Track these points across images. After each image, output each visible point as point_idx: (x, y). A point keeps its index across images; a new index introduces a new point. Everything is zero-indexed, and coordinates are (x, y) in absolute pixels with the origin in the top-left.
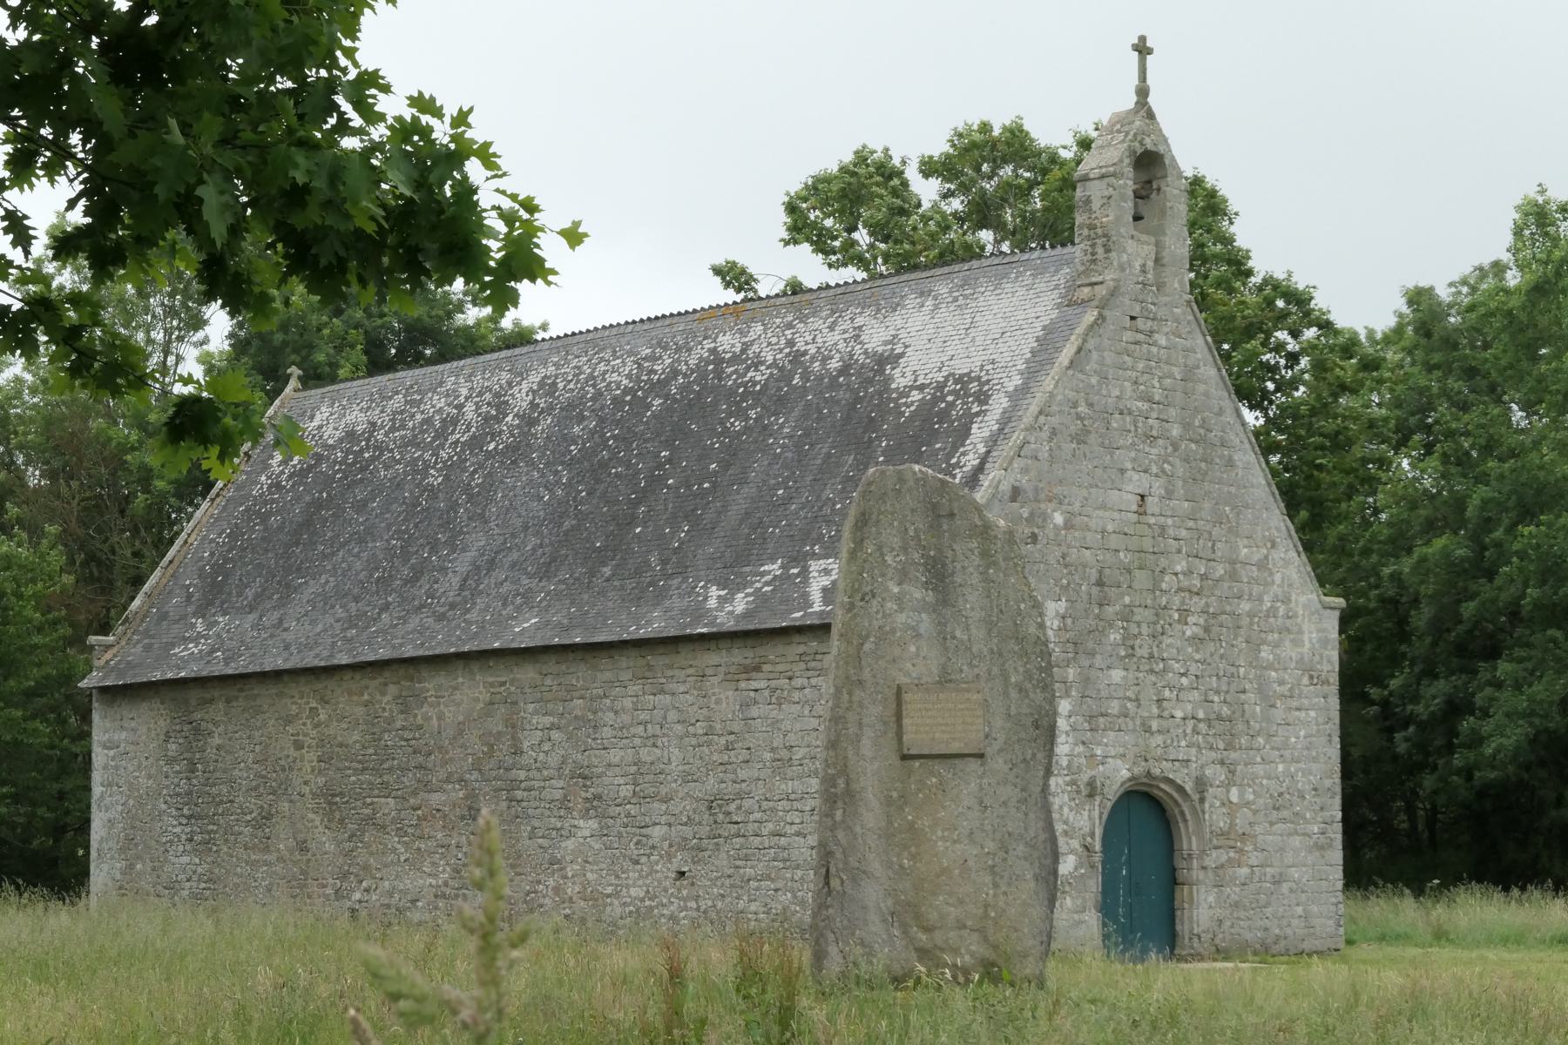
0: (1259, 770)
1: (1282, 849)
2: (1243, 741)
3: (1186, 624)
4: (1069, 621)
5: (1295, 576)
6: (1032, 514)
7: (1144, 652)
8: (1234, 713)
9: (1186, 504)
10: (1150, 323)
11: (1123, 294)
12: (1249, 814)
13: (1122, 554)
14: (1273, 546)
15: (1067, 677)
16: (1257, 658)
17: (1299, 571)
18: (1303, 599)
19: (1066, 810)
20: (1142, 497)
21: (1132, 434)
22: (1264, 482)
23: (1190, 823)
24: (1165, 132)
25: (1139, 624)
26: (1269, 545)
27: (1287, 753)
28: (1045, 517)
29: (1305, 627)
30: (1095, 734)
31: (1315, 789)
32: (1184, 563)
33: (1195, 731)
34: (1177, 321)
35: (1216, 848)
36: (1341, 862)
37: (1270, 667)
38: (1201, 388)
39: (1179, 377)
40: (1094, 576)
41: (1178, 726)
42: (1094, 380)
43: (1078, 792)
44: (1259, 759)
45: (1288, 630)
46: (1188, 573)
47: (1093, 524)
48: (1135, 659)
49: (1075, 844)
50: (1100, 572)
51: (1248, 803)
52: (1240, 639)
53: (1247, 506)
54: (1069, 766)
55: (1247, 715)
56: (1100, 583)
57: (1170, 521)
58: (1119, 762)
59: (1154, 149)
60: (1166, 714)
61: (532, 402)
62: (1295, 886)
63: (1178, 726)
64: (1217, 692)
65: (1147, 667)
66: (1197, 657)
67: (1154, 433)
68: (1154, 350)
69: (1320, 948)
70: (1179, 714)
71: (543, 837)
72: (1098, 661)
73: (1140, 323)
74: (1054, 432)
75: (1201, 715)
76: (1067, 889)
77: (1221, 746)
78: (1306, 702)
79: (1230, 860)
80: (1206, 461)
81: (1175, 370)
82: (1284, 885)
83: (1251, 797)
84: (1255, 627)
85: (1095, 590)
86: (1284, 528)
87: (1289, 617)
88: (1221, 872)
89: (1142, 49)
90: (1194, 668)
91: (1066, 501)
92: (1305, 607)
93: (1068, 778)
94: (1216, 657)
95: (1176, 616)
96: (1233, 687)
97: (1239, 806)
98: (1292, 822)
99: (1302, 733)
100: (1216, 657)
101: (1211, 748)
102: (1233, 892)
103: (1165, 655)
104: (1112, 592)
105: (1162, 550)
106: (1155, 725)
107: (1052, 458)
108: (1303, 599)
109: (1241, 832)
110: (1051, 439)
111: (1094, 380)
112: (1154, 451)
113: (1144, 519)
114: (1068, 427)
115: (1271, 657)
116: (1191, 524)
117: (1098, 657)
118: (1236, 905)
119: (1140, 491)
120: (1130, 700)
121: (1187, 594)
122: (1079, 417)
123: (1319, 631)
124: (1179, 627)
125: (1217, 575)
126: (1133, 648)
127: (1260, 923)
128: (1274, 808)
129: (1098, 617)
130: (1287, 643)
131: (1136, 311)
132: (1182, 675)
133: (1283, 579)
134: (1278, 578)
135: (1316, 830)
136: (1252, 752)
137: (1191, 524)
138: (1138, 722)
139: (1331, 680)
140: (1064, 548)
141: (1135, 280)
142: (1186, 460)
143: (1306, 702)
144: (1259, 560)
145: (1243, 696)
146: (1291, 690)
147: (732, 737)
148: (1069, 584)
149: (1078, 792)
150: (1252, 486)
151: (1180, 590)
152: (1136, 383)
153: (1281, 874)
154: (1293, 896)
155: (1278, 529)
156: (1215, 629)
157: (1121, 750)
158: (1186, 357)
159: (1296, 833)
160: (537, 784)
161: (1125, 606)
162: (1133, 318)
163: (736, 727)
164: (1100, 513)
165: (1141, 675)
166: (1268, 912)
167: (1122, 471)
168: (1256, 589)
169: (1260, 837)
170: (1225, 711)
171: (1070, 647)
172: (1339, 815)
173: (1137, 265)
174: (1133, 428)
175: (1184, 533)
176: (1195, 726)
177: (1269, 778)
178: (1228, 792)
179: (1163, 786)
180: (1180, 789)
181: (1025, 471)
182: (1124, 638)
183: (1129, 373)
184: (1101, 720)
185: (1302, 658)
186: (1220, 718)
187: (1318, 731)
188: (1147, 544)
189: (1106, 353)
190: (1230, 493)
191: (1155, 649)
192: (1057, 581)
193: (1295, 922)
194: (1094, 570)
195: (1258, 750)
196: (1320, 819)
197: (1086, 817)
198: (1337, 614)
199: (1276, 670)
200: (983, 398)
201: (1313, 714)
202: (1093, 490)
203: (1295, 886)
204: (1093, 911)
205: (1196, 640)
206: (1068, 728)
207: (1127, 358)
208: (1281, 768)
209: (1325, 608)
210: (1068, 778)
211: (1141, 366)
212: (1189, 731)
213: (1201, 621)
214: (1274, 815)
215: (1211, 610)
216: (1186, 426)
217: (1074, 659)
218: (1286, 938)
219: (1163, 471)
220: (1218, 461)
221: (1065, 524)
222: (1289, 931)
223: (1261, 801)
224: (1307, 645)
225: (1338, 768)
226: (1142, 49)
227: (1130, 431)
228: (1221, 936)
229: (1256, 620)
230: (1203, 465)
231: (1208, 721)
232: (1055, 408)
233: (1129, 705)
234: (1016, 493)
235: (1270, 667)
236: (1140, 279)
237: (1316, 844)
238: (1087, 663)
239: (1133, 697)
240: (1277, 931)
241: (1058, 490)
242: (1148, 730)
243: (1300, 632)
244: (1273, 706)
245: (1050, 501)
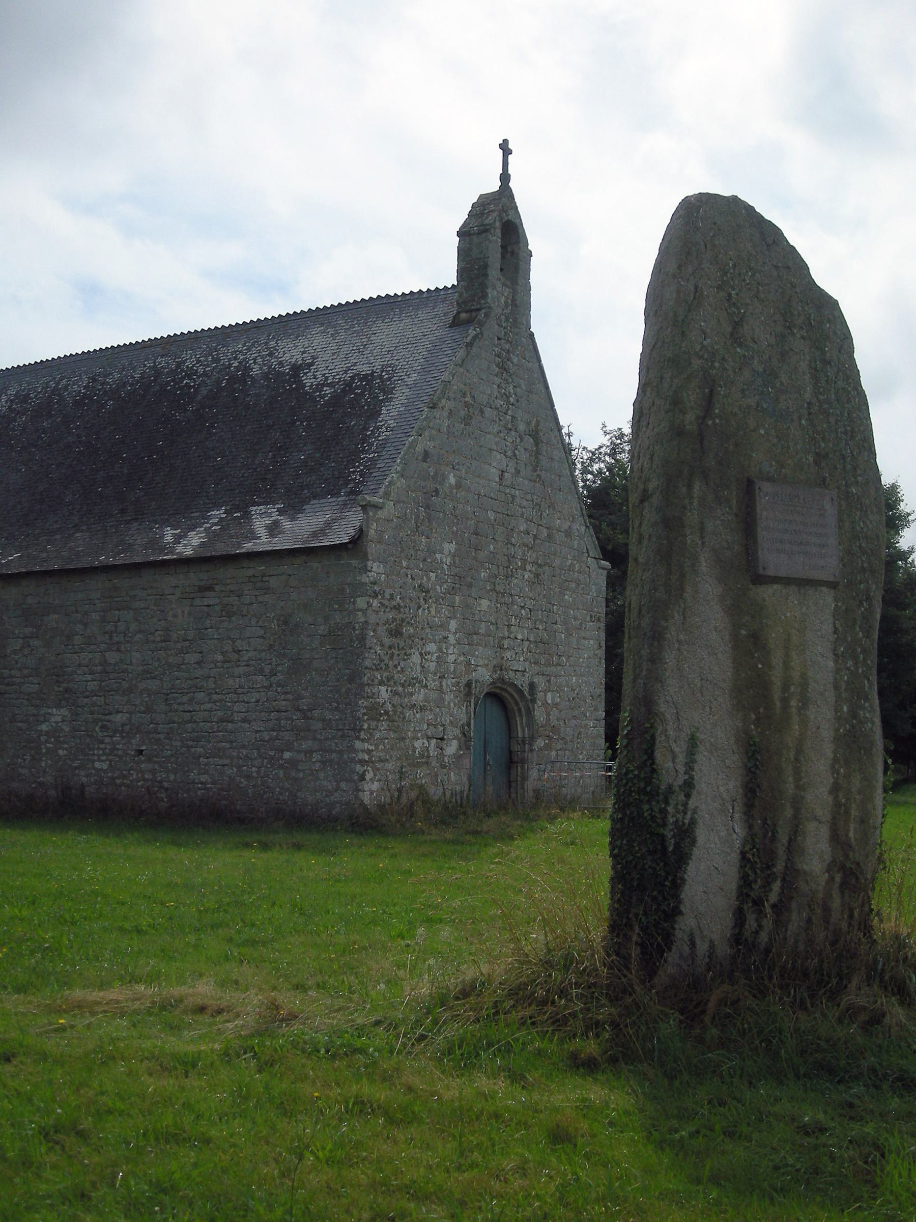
6: (436, 473)
15: (454, 603)
19: (452, 705)
23: (524, 718)
28: (444, 478)
31: (591, 696)
49: (457, 732)
60: (512, 636)
61: (10, 407)
70: (520, 637)
71: (22, 722)
75: (532, 639)
89: (505, 148)
90: (529, 604)
93: (453, 681)
94: (541, 596)
100: (541, 596)
106: (506, 643)
119: (501, 468)
136: (559, 668)
146: (581, 624)
147: (187, 644)
149: (460, 692)
160: (18, 680)
163: (191, 634)
175: (525, 503)
178: (546, 696)
181: (431, 438)
182: (489, 576)
184: (475, 637)
200: (388, 391)
201: (592, 642)
221: (456, 485)
226: (505, 148)
234: (426, 455)
242: (501, 647)
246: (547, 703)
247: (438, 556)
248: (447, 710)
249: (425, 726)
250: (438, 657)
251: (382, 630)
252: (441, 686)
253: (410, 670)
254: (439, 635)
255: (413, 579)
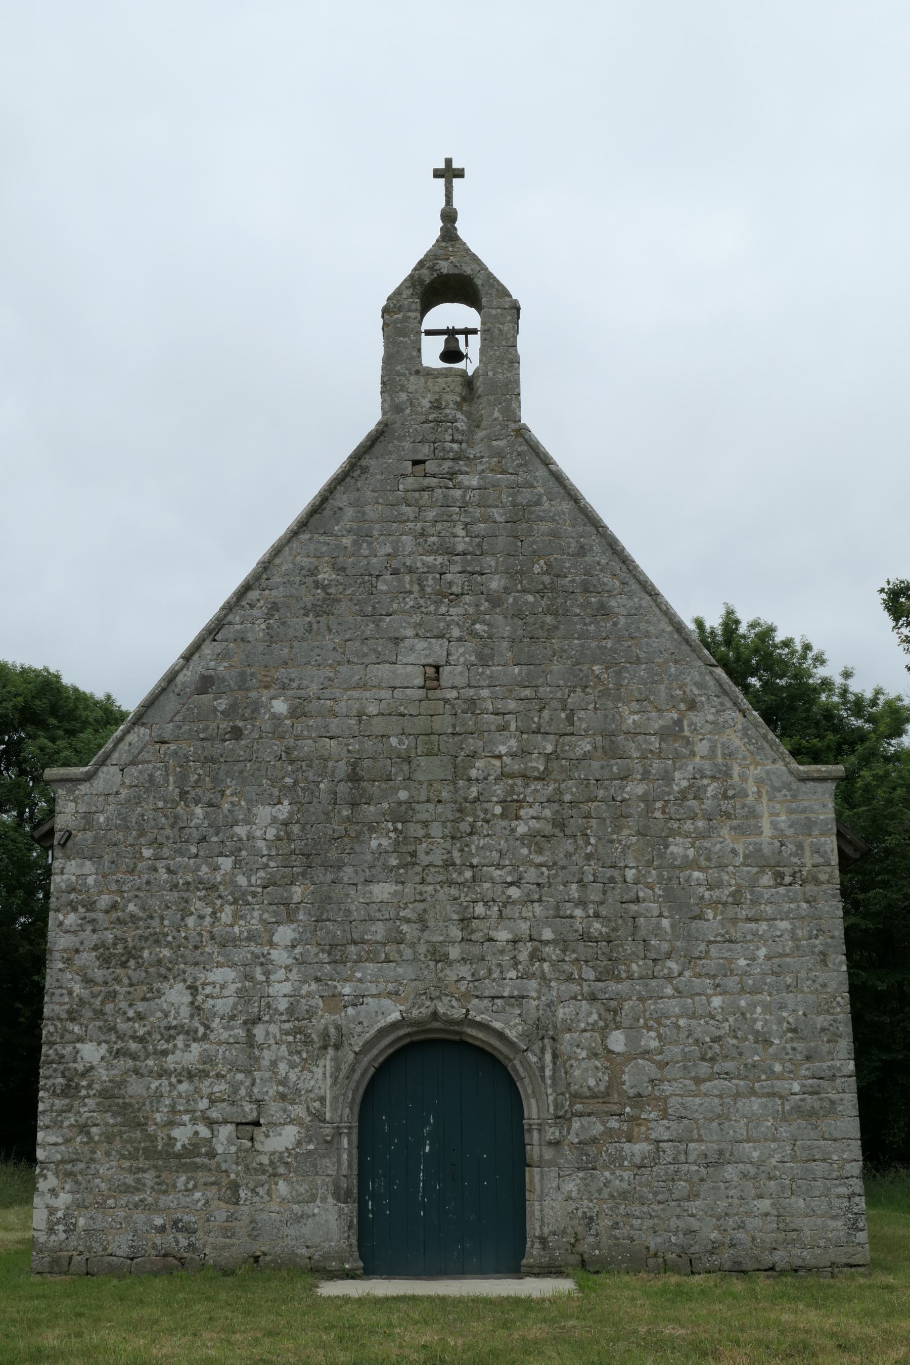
0: (674, 1006)
1: (722, 1118)
2: (634, 967)
3: (518, 818)
4: (296, 829)
5: (737, 742)
6: (233, 707)
7: (437, 858)
8: (615, 930)
9: (517, 669)
10: (449, 463)
11: (401, 439)
12: (651, 1069)
13: (394, 741)
14: (692, 705)
16: (661, 856)
17: (745, 734)
18: (755, 772)
19: (283, 1067)
20: (437, 668)
21: (416, 595)
22: (669, 629)
23: (527, 1080)
24: (474, 250)
25: (425, 824)
26: (683, 706)
27: (732, 982)
29: (764, 808)
30: (340, 967)
31: (794, 1031)
32: (513, 743)
33: (535, 956)
34: (500, 454)
35: (581, 1115)
36: (859, 1135)
37: (693, 865)
38: (544, 527)
39: (499, 519)
40: (342, 769)
41: (502, 952)
42: (347, 541)
43: (308, 1042)
44: (669, 991)
45: (728, 816)
46: (523, 753)
47: (342, 707)
48: (418, 869)
49: (299, 1111)
50: (354, 766)
51: (648, 1052)
52: (626, 832)
53: (638, 661)
54: (291, 1010)
55: (643, 933)
56: (354, 777)
57: (485, 693)
58: (386, 1002)
59: (456, 271)
62: (752, 1170)
63: (502, 952)
64: (582, 903)
65: (441, 878)
66: (539, 859)
67: (455, 589)
68: (458, 493)
69: (812, 1262)
70: (503, 935)
72: (348, 873)
73: (431, 467)
74: (274, 607)
75: (547, 934)
76: (281, 1170)
77: (591, 975)
78: (769, 909)
79: (609, 1133)
80: (555, 614)
81: (497, 514)
82: (729, 1168)
83: (654, 1044)
84: (658, 814)
85: (343, 788)
86: (711, 683)
87: (725, 797)
88: (592, 1150)
90: (531, 875)
91: (295, 685)
92: (759, 782)
93: (287, 1026)
95: (498, 810)
96: (614, 896)
97: (628, 1057)
98: (745, 1078)
99: (762, 952)
101: (569, 979)
102: (622, 1179)
103: (475, 861)
104: (375, 789)
105: (472, 728)
106: (454, 952)
107: (271, 638)
108: (755, 772)
109: (631, 1092)
110: (270, 615)
111: (347, 541)
112: (453, 611)
113: (438, 694)
114: (298, 599)
115: (691, 853)
116: (528, 692)
117: (349, 870)
118: (624, 1195)
120: (408, 921)
121: (519, 781)
122: (317, 585)
123: (791, 812)
124: (504, 823)
125: (579, 752)
126: (413, 854)
127: (674, 1222)
128: (703, 1059)
129: (348, 819)
130: (725, 831)
131: (424, 451)
132: (511, 884)
133: (713, 750)
134: (702, 748)
135: (796, 1087)
136: (654, 983)
137: (528, 692)
138: (422, 949)
139: (823, 877)
140: (291, 742)
141: (423, 418)
142: (519, 615)
143: (769, 909)
144: (663, 727)
145: (633, 907)
148: (296, 782)
150: (647, 635)
151: (503, 775)
152: (422, 535)
153: (721, 1153)
154: (750, 1184)
155: (700, 685)
156: (577, 822)
157: (390, 987)
158: (514, 495)
159: (753, 1092)
161: (400, 803)
162: (415, 463)
164: (356, 694)
165: (430, 888)
166: (694, 1206)
167: (397, 640)
168: (656, 766)
169: (672, 1101)
170: (597, 927)
171: (297, 861)
172: (851, 1065)
173: (426, 403)
174: (416, 588)
175: (512, 705)
176: (535, 950)
177: (693, 1016)
178: (604, 1038)
179: (470, 1031)
180: (501, 1035)
182: (397, 843)
183: (410, 525)
184: (352, 949)
185: (760, 850)
186: (586, 937)
187: (798, 948)
188: (443, 723)
189: (368, 509)
190: (600, 647)
191: (456, 854)
192: (273, 782)
193: (753, 1223)
194: (342, 764)
195: (669, 978)
196: (804, 1072)
197: (320, 1076)
198: (831, 786)
199: (700, 869)
201: (784, 925)
202: (343, 669)
203: (752, 1170)
204: (331, 1200)
205: (535, 839)
206: (290, 961)
207: (404, 509)
208: (717, 1002)
209: (803, 780)
210: (287, 1026)
211: (431, 514)
212: (523, 956)
213: (547, 813)
214: (704, 1068)
215: (567, 798)
216: (515, 575)
217: (303, 874)
218: (732, 1246)
219: (473, 634)
220: (578, 611)
222: (741, 1235)
223: (676, 1049)
224: (767, 831)
225: (844, 999)
227: (411, 592)
228: (591, 1240)
229: (659, 805)
230: (549, 619)
231: (562, 943)
232: (277, 579)
233: (405, 928)
235: (693, 865)
236: (431, 417)
237: (797, 1109)
238: (329, 877)
239: (413, 916)
240: (714, 1235)
241: (281, 673)
243: (753, 814)
244: (700, 917)
245: (266, 687)
246: (611, 1052)
247: (241, 831)
248: (267, 1075)
249: (203, 1104)
250: (238, 991)
251: (86, 958)
252: (250, 1036)
253: (159, 1014)
254: (241, 954)
255: (169, 871)
